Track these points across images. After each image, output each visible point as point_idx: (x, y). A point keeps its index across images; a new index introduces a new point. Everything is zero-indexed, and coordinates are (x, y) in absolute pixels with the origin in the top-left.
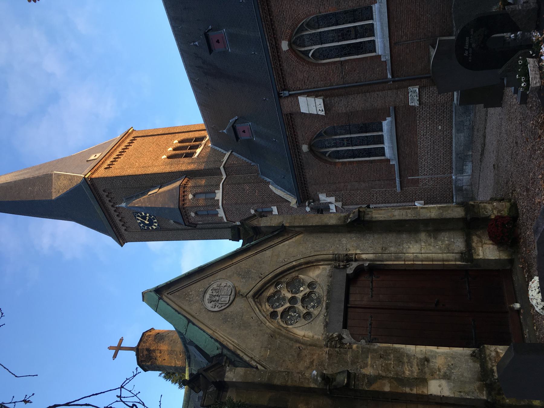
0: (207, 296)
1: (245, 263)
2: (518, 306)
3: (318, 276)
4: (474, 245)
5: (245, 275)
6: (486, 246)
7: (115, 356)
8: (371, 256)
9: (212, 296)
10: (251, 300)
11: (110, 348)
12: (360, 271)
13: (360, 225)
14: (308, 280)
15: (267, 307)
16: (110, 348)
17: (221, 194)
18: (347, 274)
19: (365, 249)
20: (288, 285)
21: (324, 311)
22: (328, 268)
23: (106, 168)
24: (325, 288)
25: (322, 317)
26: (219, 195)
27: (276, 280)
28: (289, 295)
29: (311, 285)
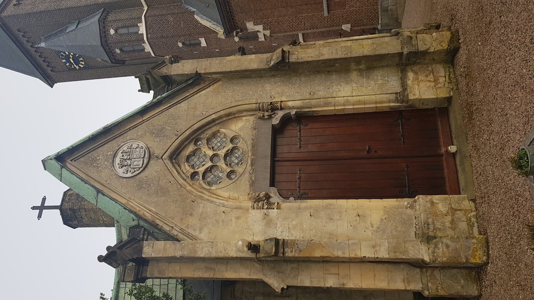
0: (117, 160)
1: (159, 119)
2: (453, 149)
3: (241, 129)
4: (409, 82)
5: (159, 133)
6: (422, 85)
7: (40, 216)
8: (298, 103)
9: (123, 160)
10: (168, 162)
11: (34, 208)
12: (286, 120)
13: (285, 69)
15: (187, 168)
16: (34, 208)
17: (144, 27)
18: (273, 126)
19: (292, 96)
21: (249, 168)
22: (252, 119)
23: (15, 5)
24: (250, 142)
25: (247, 175)
26: (142, 29)
27: (194, 137)
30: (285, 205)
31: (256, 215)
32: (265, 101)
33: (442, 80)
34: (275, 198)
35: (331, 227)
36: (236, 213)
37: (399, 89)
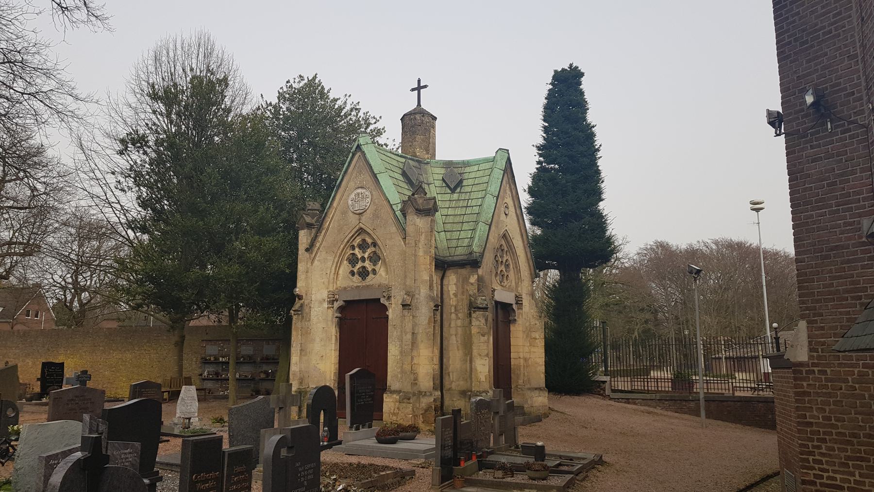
0: (359, 191)
1: (386, 212)
3: (381, 275)
4: (395, 396)
5: (376, 216)
6: (392, 404)
8: (390, 317)
14: (377, 269)
15: (358, 240)
20: (375, 253)
21: (355, 285)
24: (371, 283)
25: (351, 284)
28: (366, 256)
29: (374, 272)
30: (330, 312)
31: (324, 294)
32: (393, 292)
33: (394, 418)
34: (336, 305)
35: (318, 340)
36: (326, 280)
37: (393, 388)
